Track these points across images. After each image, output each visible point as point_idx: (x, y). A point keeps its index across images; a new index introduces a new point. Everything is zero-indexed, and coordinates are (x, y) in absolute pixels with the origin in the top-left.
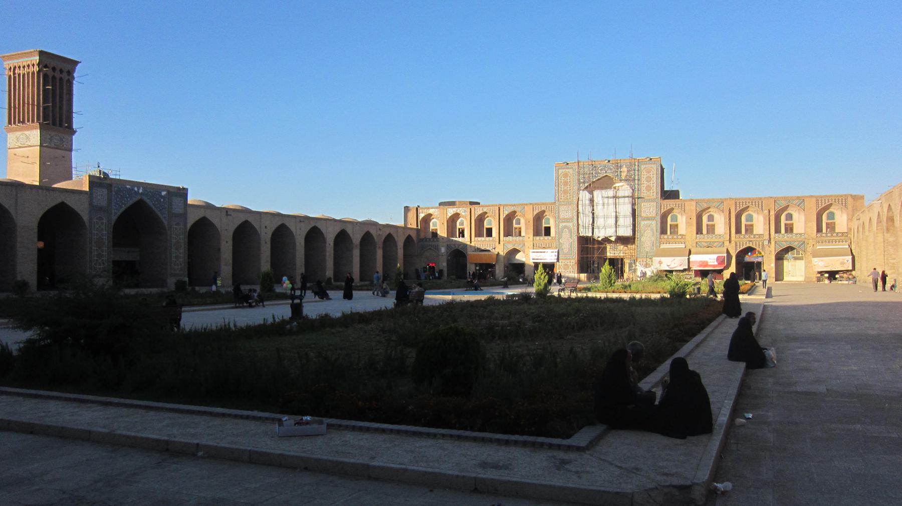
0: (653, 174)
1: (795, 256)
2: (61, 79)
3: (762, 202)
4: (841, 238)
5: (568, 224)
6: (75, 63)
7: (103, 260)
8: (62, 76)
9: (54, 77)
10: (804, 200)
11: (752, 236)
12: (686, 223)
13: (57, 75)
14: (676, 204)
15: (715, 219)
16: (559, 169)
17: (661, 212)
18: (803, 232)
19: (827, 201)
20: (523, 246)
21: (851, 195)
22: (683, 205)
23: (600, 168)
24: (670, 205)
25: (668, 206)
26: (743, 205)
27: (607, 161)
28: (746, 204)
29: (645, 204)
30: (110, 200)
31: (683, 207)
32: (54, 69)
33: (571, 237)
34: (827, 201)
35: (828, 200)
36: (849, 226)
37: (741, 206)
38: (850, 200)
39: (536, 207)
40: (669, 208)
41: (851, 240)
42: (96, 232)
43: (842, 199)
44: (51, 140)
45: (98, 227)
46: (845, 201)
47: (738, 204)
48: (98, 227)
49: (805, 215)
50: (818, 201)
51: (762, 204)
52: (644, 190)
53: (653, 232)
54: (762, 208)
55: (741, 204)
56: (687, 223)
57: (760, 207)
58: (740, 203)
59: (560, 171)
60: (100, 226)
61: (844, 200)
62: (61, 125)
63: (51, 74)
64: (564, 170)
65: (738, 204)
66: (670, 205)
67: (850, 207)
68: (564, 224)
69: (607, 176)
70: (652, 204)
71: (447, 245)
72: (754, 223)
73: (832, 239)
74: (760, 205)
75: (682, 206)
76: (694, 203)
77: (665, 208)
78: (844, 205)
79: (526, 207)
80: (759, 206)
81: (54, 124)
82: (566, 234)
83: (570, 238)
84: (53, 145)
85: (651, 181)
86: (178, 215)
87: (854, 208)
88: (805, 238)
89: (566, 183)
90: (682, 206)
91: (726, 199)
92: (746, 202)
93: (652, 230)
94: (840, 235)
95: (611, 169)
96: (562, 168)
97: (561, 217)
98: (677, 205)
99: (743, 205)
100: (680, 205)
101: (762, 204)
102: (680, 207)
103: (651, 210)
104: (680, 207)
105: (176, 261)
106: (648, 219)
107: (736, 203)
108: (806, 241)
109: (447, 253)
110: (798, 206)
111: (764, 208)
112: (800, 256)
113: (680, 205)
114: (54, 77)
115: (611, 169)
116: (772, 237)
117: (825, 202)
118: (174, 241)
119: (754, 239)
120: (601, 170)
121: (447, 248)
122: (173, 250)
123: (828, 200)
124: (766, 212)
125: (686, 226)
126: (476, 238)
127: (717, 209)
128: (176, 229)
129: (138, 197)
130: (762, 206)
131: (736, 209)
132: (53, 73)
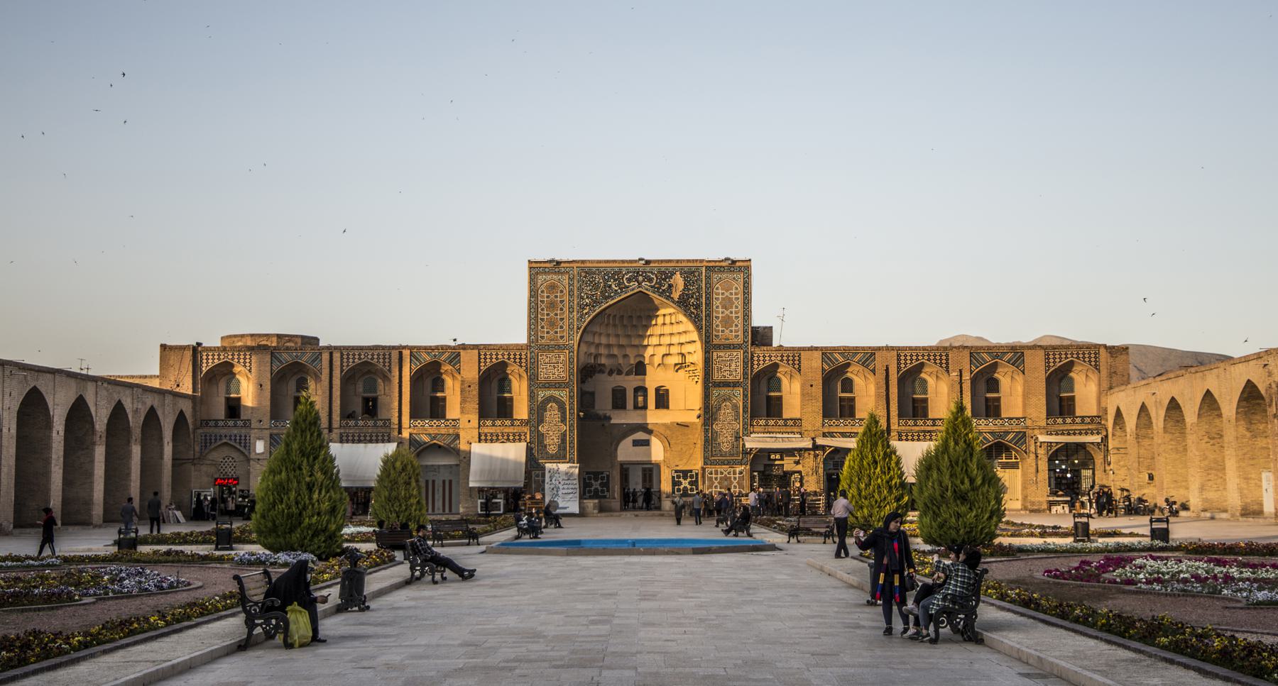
0: (736, 294)
1: (1004, 460)
3: (947, 355)
4: (1090, 427)
5: (556, 393)
10: (1023, 353)
12: (803, 395)
14: (782, 356)
15: (856, 388)
16: (537, 273)
17: (752, 371)
18: (1020, 415)
19: (1063, 356)
20: (454, 440)
21: (1105, 346)
22: (797, 358)
24: (770, 356)
25: (767, 358)
26: (911, 360)
27: (643, 262)
28: (917, 360)
29: (722, 354)
31: (797, 362)
33: (563, 420)
34: (1063, 356)
35: (1066, 354)
36: (1103, 405)
37: (908, 362)
38: (1103, 354)
39: (485, 355)
40: (768, 363)
41: (1107, 431)
43: (1090, 354)
46: (1095, 358)
49: (1025, 381)
50: (1048, 355)
52: (717, 326)
53: (738, 412)
54: (947, 367)
55: (908, 358)
56: (804, 394)
57: (944, 365)
58: (905, 356)
59: (541, 278)
61: (1093, 356)
64: (549, 277)
65: (903, 358)
66: (770, 356)
67: (1104, 372)
68: (548, 393)
69: (641, 291)
70: (736, 353)
71: (271, 435)
72: (930, 395)
73: (1074, 428)
74: (944, 361)
75: (794, 360)
76: (818, 354)
77: (761, 362)
78: (1093, 363)
79: (462, 353)
80: (941, 363)
82: (552, 413)
83: (562, 421)
85: (732, 308)
87: (1112, 371)
88: (1027, 427)
89: (552, 305)
90: (794, 360)
91: (879, 349)
92: (917, 356)
93: (735, 407)
94: (1088, 420)
95: (650, 280)
96: (545, 273)
97: (542, 376)
98: (785, 358)
99: (911, 360)
100: (791, 358)
102: (791, 362)
106: (726, 384)
107: (899, 356)
108: (1029, 432)
109: (271, 453)
110: (1013, 364)
111: (950, 369)
112: (1014, 460)
113: (791, 358)
115: (650, 280)
117: (1060, 358)
119: (935, 428)
120: (629, 280)
121: (271, 444)
123: (1066, 354)
124: (955, 374)
125: (802, 401)
126: (344, 423)
127: (861, 368)
130: (947, 364)
131: (899, 368)
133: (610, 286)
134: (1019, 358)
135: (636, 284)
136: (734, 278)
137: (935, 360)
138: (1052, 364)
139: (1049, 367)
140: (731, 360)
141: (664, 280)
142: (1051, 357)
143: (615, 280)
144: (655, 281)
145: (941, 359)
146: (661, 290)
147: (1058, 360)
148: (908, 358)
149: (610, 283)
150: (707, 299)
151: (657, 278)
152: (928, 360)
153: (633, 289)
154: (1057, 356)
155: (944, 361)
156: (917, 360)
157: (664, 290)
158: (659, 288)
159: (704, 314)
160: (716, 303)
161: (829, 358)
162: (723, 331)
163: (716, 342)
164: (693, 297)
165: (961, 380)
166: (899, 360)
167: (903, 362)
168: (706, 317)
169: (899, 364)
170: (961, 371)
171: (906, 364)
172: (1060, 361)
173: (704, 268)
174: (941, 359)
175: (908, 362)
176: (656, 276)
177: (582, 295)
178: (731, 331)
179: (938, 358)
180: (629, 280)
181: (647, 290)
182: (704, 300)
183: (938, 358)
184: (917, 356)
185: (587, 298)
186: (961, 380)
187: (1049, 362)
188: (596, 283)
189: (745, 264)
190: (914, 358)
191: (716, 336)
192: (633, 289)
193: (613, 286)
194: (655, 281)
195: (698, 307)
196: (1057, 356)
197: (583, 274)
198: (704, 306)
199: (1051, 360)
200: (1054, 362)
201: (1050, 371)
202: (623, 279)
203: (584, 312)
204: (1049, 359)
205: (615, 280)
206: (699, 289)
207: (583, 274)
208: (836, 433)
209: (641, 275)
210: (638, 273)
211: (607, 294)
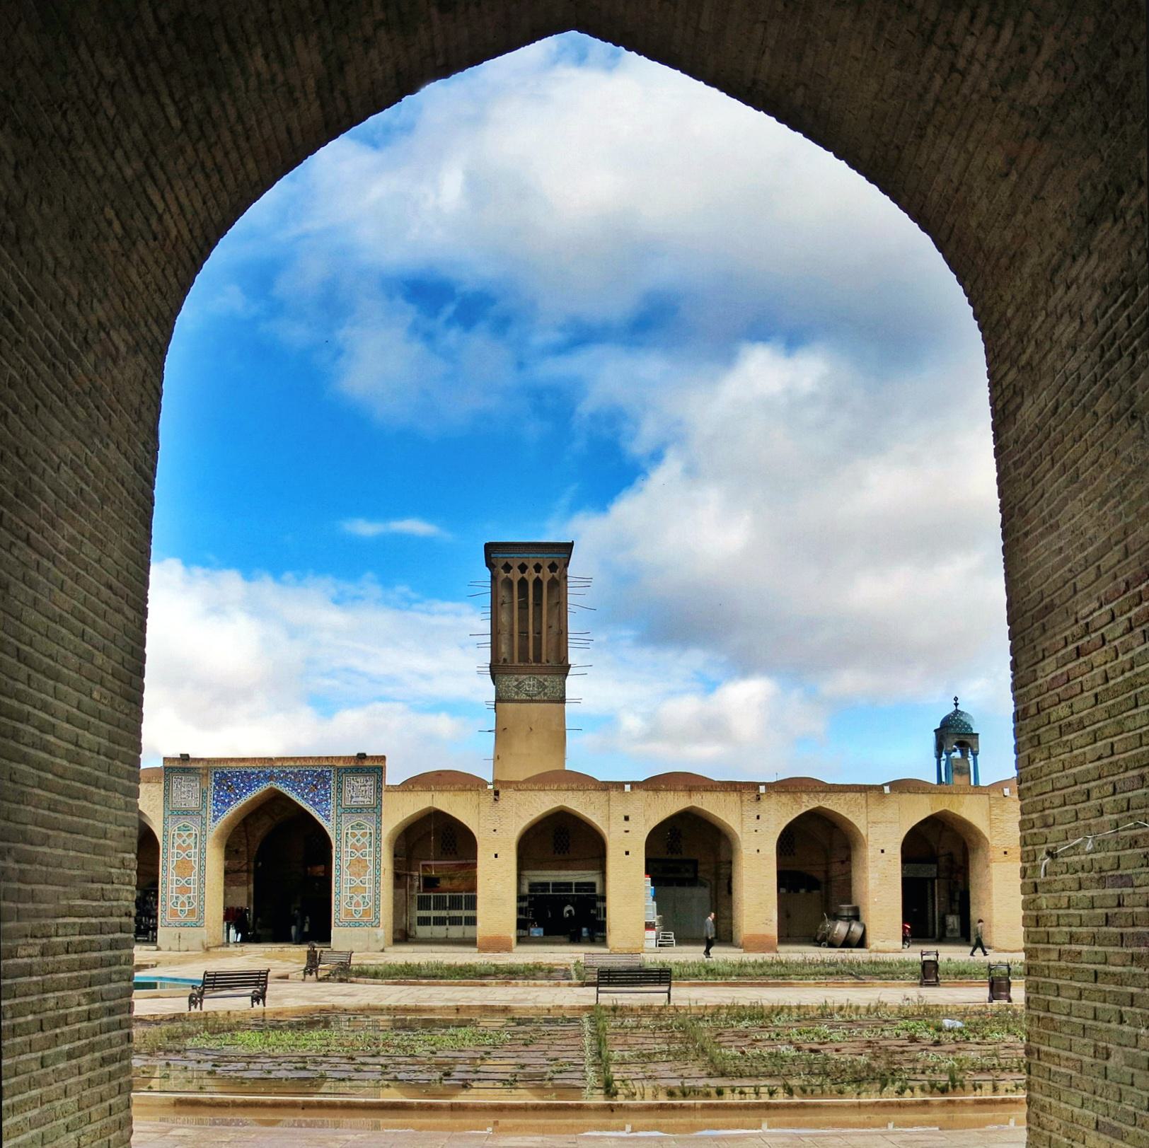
2: (538, 582)
6: (568, 547)
7: (189, 898)
8: (540, 575)
9: (523, 583)
13: (531, 575)
30: (340, 790)
32: (523, 568)
42: (176, 851)
44: (519, 688)
45: (180, 841)
48: (180, 841)
60: (184, 842)
62: (538, 658)
63: (515, 575)
81: (524, 657)
84: (524, 697)
86: (359, 810)
105: (351, 898)
114: (523, 583)
118: (346, 859)
122: (346, 876)
128: (354, 835)
129: (265, 787)
132: (520, 576)
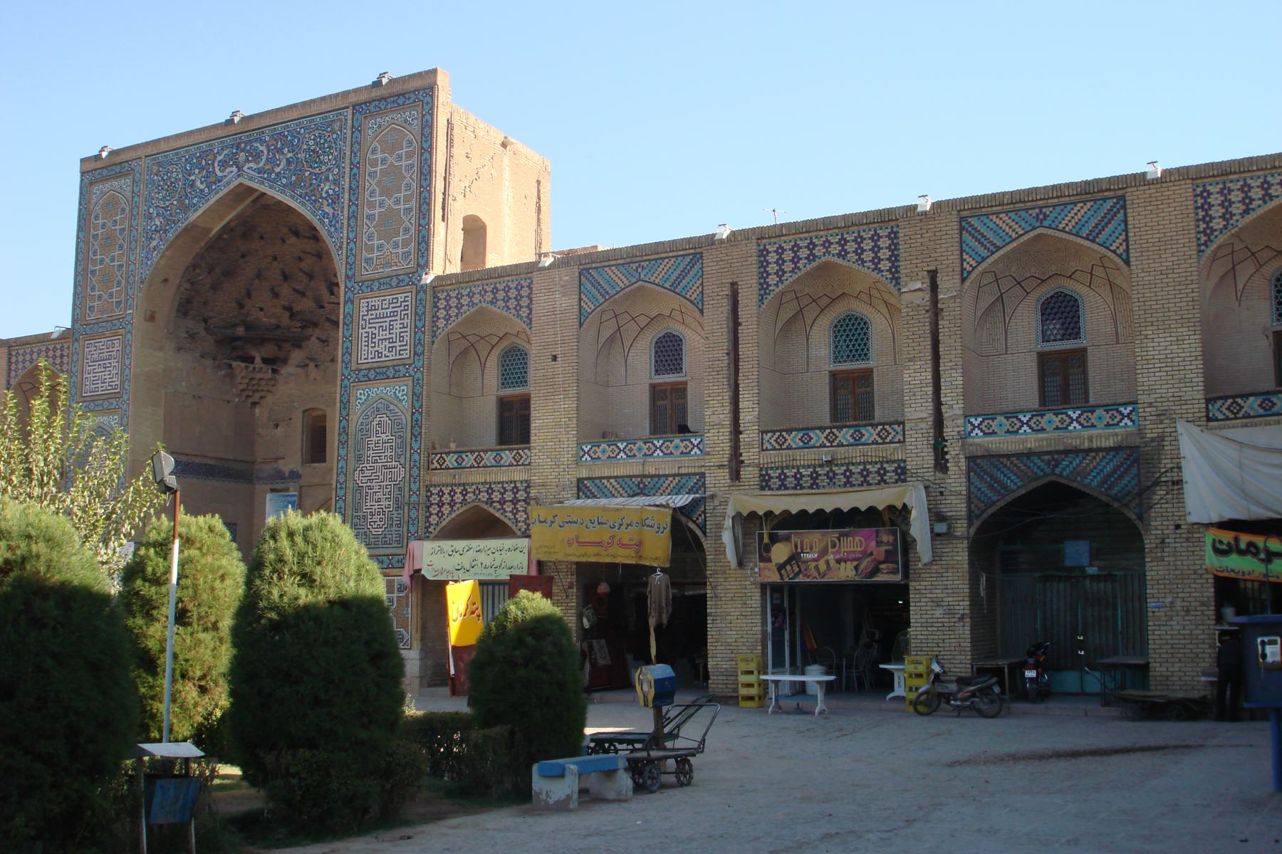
0: (409, 156)
3: (893, 236)
10: (1123, 198)
11: (870, 434)
19: (1256, 193)
23: (219, 158)
26: (796, 259)
28: (811, 257)
29: (375, 302)
34: (1256, 193)
47: (772, 258)
50: (1205, 194)
51: (894, 248)
52: (370, 237)
54: (894, 272)
55: (788, 255)
57: (885, 265)
65: (772, 258)
70: (401, 297)
74: (884, 254)
80: (876, 261)
95: (257, 156)
101: (894, 248)
103: (397, 325)
104: (512, 303)
106: (380, 373)
107: (763, 253)
115: (257, 156)
116: (950, 431)
117: (1247, 201)
130: (894, 258)
131: (764, 288)
133: (192, 185)
134: (1111, 215)
135: (235, 169)
136: (406, 121)
137: (859, 252)
138: (1218, 224)
139: (1209, 232)
140: (394, 314)
141: (280, 151)
142: (1215, 199)
143: (202, 169)
144: (264, 158)
145: (876, 249)
146: (273, 176)
147: (1237, 209)
148: (788, 255)
149: (193, 178)
150: (353, 177)
151: (268, 152)
152: (839, 255)
153: (229, 183)
154: (1236, 196)
155: (884, 254)
156: (811, 257)
157: (278, 174)
158: (270, 172)
159: (346, 212)
160: (371, 184)
161: (595, 284)
162: (380, 247)
163: (367, 273)
164: (327, 179)
165: (935, 301)
166: (763, 265)
167: (772, 268)
168: (349, 219)
169: (764, 275)
170: (933, 275)
171: (780, 273)
172: (1246, 211)
173: (350, 111)
174: (876, 249)
175: (788, 267)
176: (268, 147)
177: (151, 210)
178: (396, 245)
179: (867, 245)
180: (224, 164)
181: (251, 179)
182: (347, 180)
183: (867, 245)
184: (810, 247)
185: (158, 215)
186: (935, 301)
187: (1207, 219)
188: (172, 183)
189: (426, 82)
190: (804, 253)
191: (367, 260)
192: (229, 183)
193: (198, 183)
194: (264, 158)
195: (335, 200)
196: (1236, 196)
197: (155, 169)
198: (346, 196)
199: (1217, 212)
200: (1227, 216)
201: (1213, 247)
202: (213, 164)
203: (152, 246)
204: (1206, 207)
205: (202, 169)
206: (341, 156)
207: (155, 169)
208: (608, 478)
209: (243, 151)
210: (238, 146)
211: (187, 202)
